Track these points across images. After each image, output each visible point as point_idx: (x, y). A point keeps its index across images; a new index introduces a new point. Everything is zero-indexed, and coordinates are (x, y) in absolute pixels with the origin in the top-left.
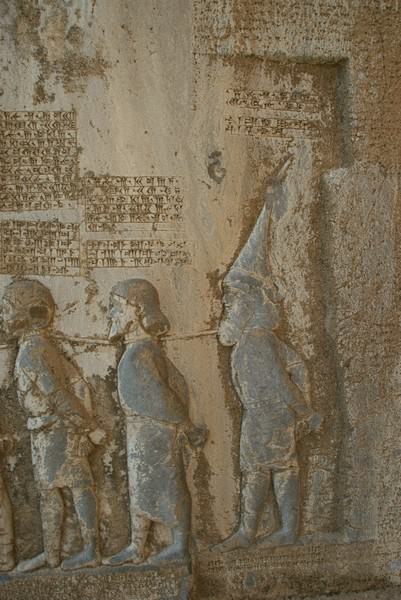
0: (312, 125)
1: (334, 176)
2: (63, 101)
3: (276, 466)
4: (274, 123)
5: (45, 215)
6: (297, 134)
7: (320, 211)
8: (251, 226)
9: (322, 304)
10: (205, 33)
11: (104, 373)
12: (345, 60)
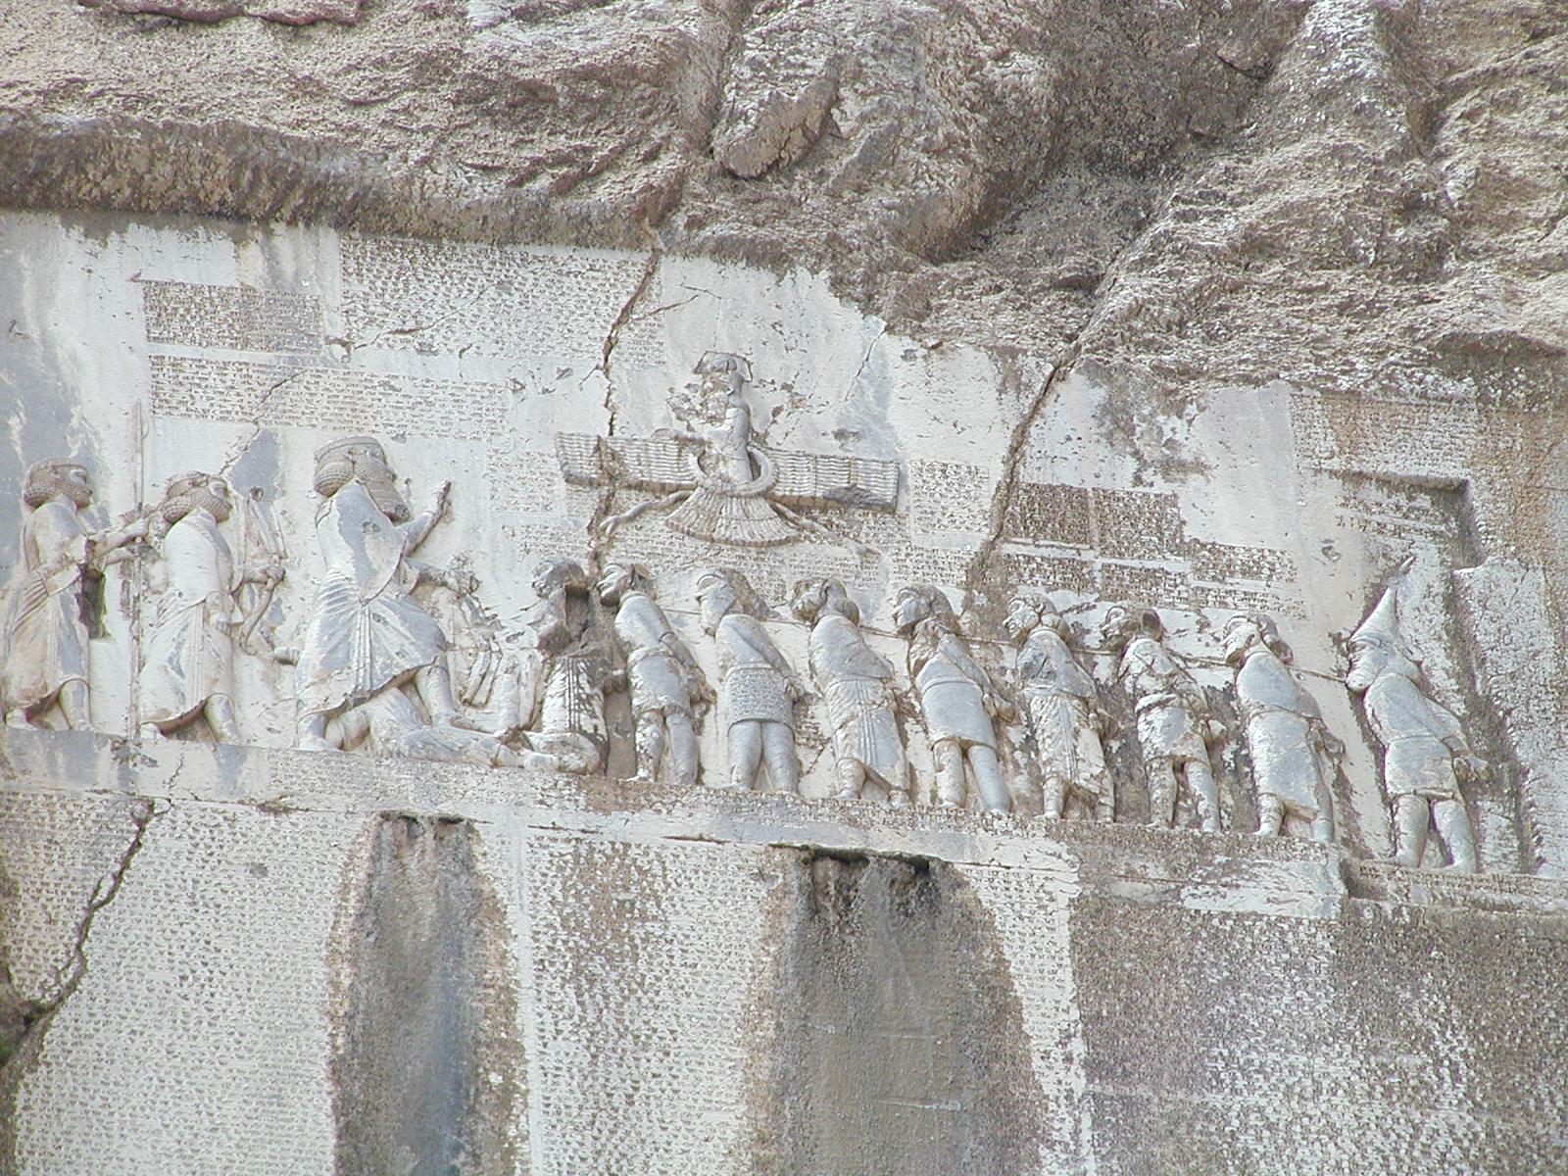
0: (1434, 534)
2: (1161, 487)
3: (1434, 792)
4: (1391, 527)
5: (1150, 565)
7: (1453, 601)
8: (1375, 606)
9: (1465, 676)
11: (1220, 686)
12: (1464, 484)
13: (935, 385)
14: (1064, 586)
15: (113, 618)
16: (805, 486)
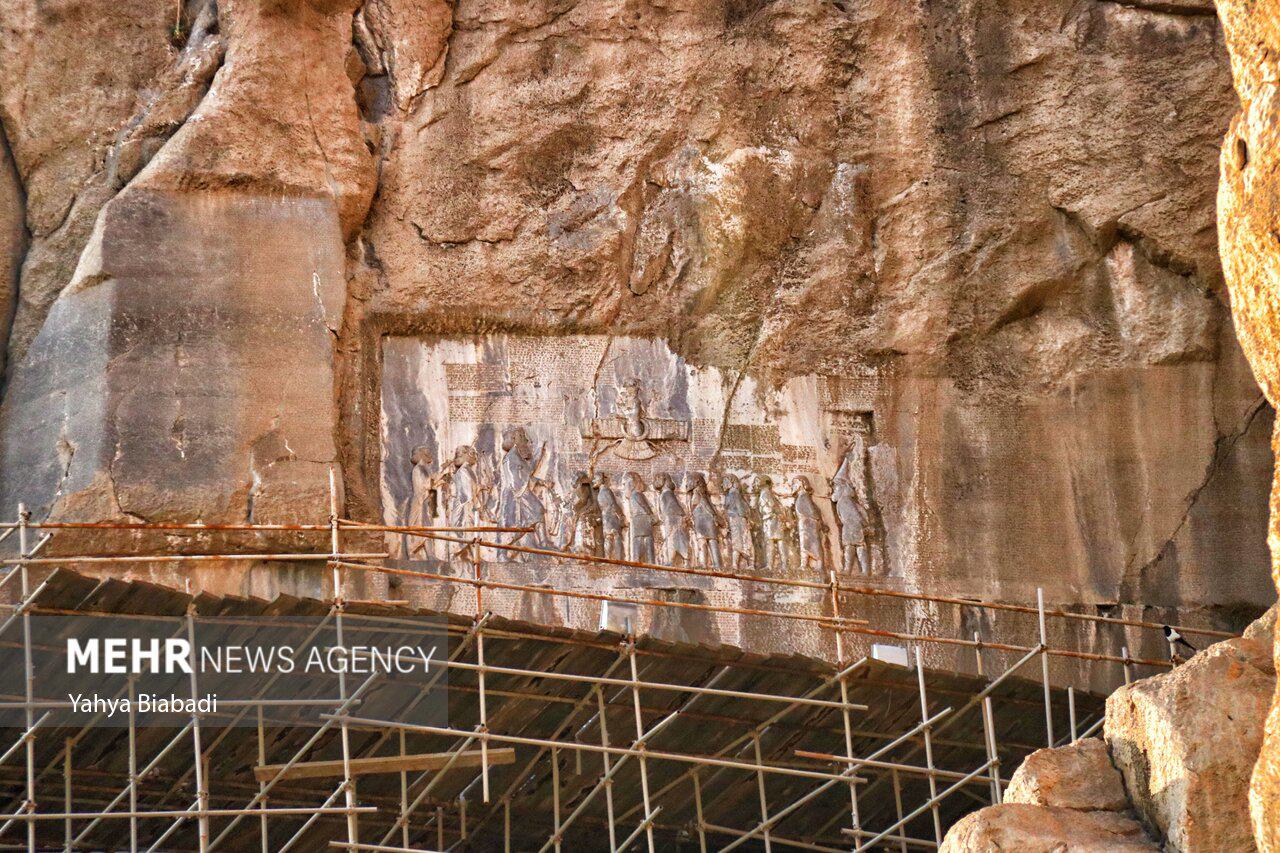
0: (863, 433)
1: (871, 449)
2: (774, 422)
6: (857, 435)
7: (867, 460)
9: (869, 492)
10: (822, 404)
15: (440, 509)
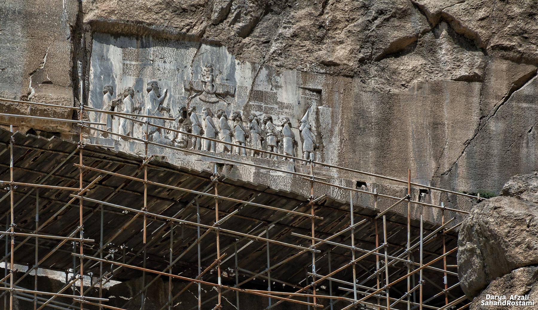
0: (316, 99)
2: (275, 91)
7: (317, 112)
10: (298, 84)
13: (242, 70)
14: (258, 111)
16: (220, 91)
